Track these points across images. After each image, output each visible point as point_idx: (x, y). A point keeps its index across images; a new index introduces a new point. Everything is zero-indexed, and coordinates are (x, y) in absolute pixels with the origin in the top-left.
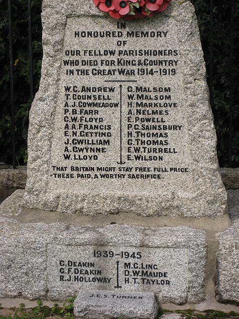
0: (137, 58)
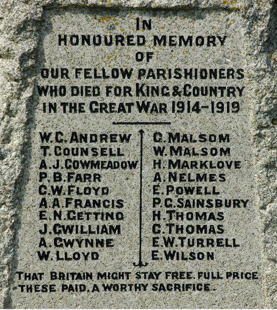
0: (171, 83)
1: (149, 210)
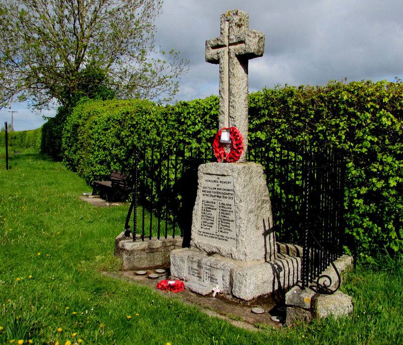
0: (222, 191)
1: (218, 220)
